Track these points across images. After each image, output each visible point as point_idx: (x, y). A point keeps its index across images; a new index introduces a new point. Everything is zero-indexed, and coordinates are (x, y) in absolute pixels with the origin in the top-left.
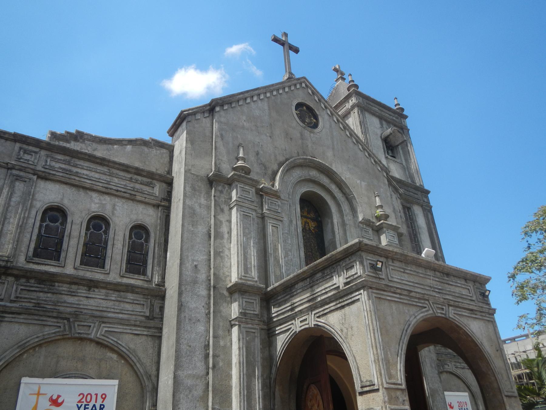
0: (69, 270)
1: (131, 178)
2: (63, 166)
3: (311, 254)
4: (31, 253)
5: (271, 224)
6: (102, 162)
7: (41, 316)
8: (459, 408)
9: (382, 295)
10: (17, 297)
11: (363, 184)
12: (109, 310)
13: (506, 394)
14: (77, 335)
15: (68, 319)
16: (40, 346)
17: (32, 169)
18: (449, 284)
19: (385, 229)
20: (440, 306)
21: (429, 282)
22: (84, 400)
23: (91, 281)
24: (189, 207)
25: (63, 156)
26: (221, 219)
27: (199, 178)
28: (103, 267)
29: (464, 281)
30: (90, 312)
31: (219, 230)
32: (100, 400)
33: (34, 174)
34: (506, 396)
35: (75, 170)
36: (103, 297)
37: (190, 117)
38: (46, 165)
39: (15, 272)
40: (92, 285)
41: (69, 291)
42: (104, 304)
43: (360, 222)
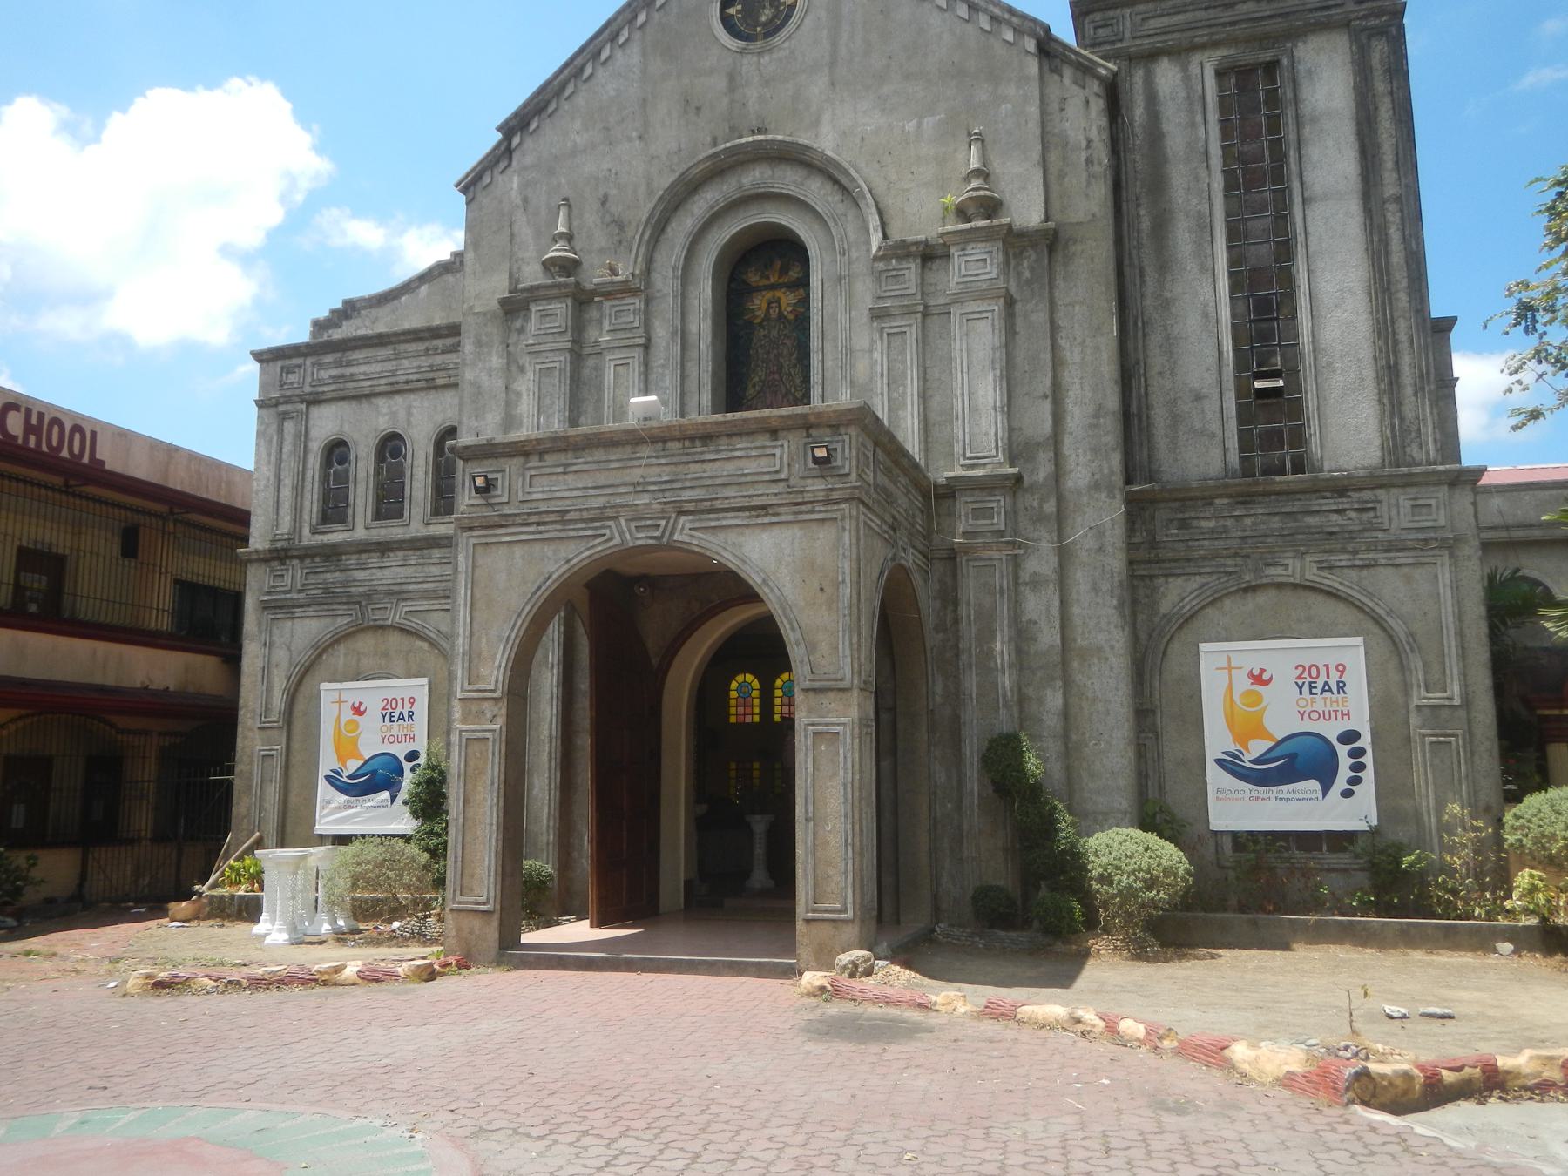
0: (360, 533)
1: (427, 349)
2: (334, 372)
3: (777, 376)
4: (314, 522)
5: (613, 363)
6: (381, 340)
7: (331, 604)
8: (1300, 682)
9: (495, 535)
10: (305, 585)
11: (929, 122)
12: (409, 580)
13: (807, 684)
14: (372, 623)
15: (359, 603)
16: (337, 641)
17: (298, 396)
18: (703, 461)
19: (953, 250)
20: (649, 522)
21: (636, 474)
22: (388, 706)
23: (379, 543)
24: (471, 384)
25: (332, 355)
26: (519, 388)
27: (489, 317)
28: (401, 515)
29: (768, 435)
30: (385, 588)
31: (514, 413)
32: (408, 706)
33: (302, 402)
34: (806, 690)
35: (348, 371)
36: (400, 563)
37: (472, 189)
38: (313, 380)
39: (295, 553)
40: (384, 548)
41: (358, 564)
42: (403, 572)
43: (876, 259)
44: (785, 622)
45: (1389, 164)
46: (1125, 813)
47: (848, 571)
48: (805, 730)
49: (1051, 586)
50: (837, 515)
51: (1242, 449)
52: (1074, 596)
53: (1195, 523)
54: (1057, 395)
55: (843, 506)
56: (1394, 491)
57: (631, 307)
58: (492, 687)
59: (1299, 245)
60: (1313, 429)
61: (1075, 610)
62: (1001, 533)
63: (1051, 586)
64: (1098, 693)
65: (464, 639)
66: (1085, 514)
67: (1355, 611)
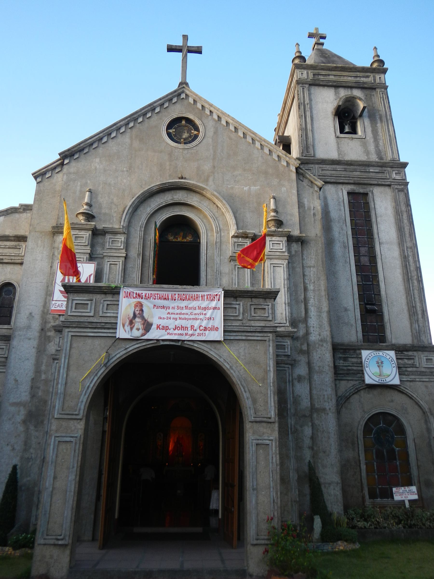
5: (109, 263)
44: (242, 388)
45: (407, 235)
46: (337, 483)
47: (272, 365)
48: (252, 443)
49: (306, 381)
50: (267, 339)
51: (363, 331)
52: (314, 386)
53: (350, 359)
54: (306, 301)
55: (269, 335)
56: (420, 353)
57: (120, 240)
58: (77, 413)
59: (379, 258)
60: (388, 326)
61: (314, 392)
62: (288, 356)
63: (306, 381)
64: (325, 429)
65: (61, 386)
66: (317, 351)
67: (409, 399)
